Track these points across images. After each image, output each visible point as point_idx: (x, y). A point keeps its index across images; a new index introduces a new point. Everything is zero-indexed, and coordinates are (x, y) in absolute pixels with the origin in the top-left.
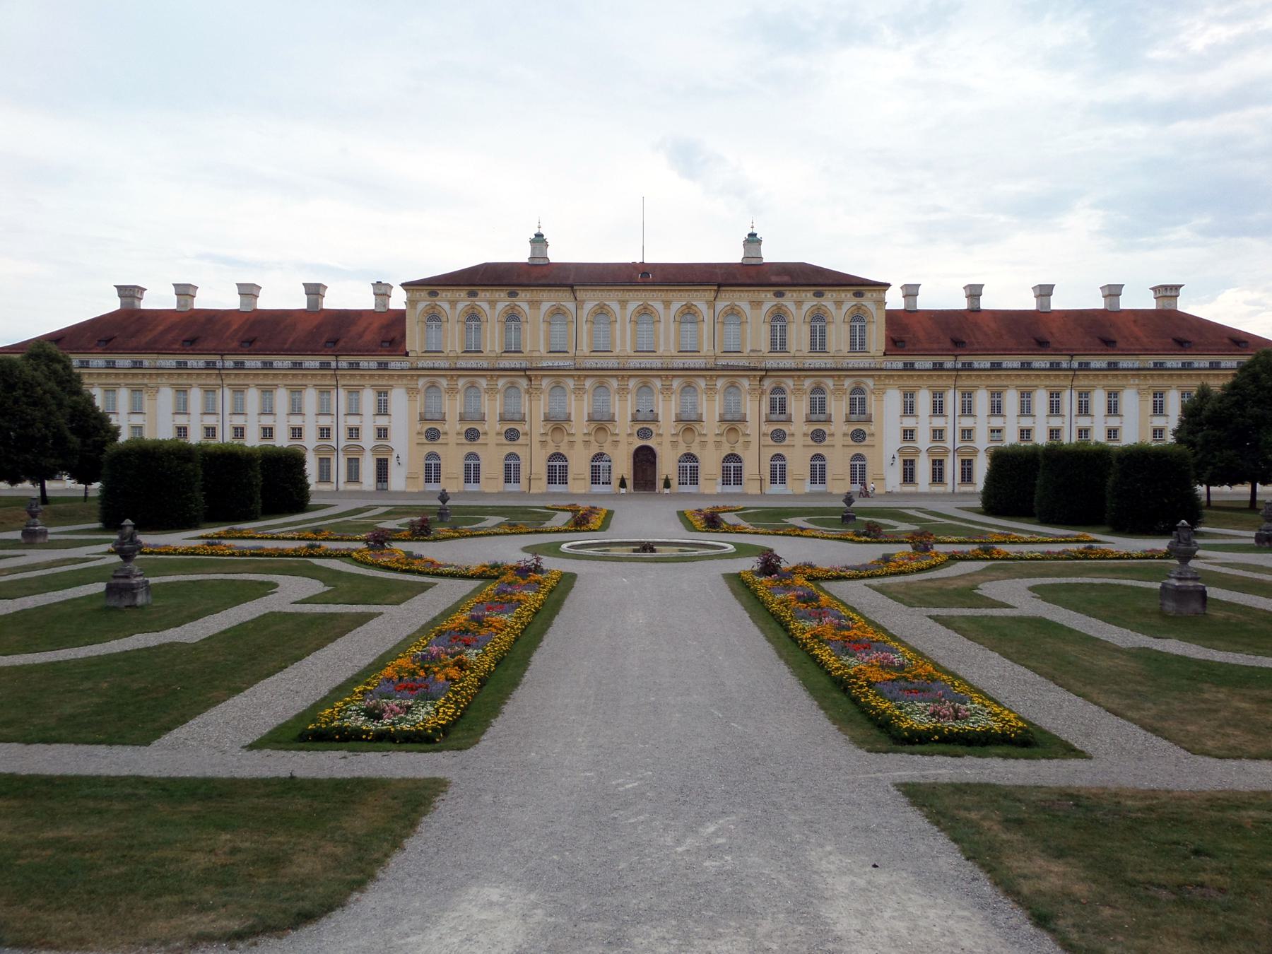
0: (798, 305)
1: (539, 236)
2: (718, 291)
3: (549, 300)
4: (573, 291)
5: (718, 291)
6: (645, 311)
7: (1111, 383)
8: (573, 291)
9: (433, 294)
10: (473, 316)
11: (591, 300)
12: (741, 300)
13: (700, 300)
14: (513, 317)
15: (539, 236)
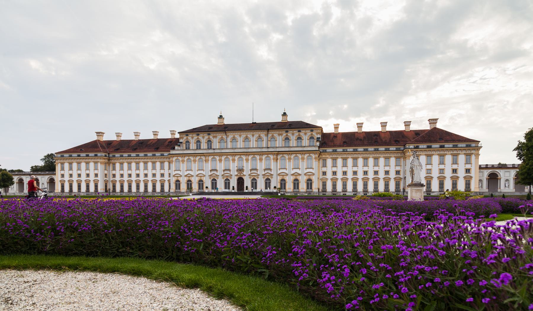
0: (293, 135)
1: (221, 116)
2: (268, 131)
3: (219, 136)
4: (226, 133)
5: (268, 131)
6: (247, 138)
7: (454, 152)
8: (226, 133)
9: (187, 135)
10: (198, 142)
11: (231, 135)
12: (275, 133)
13: (263, 134)
14: (209, 142)
15: (221, 116)
